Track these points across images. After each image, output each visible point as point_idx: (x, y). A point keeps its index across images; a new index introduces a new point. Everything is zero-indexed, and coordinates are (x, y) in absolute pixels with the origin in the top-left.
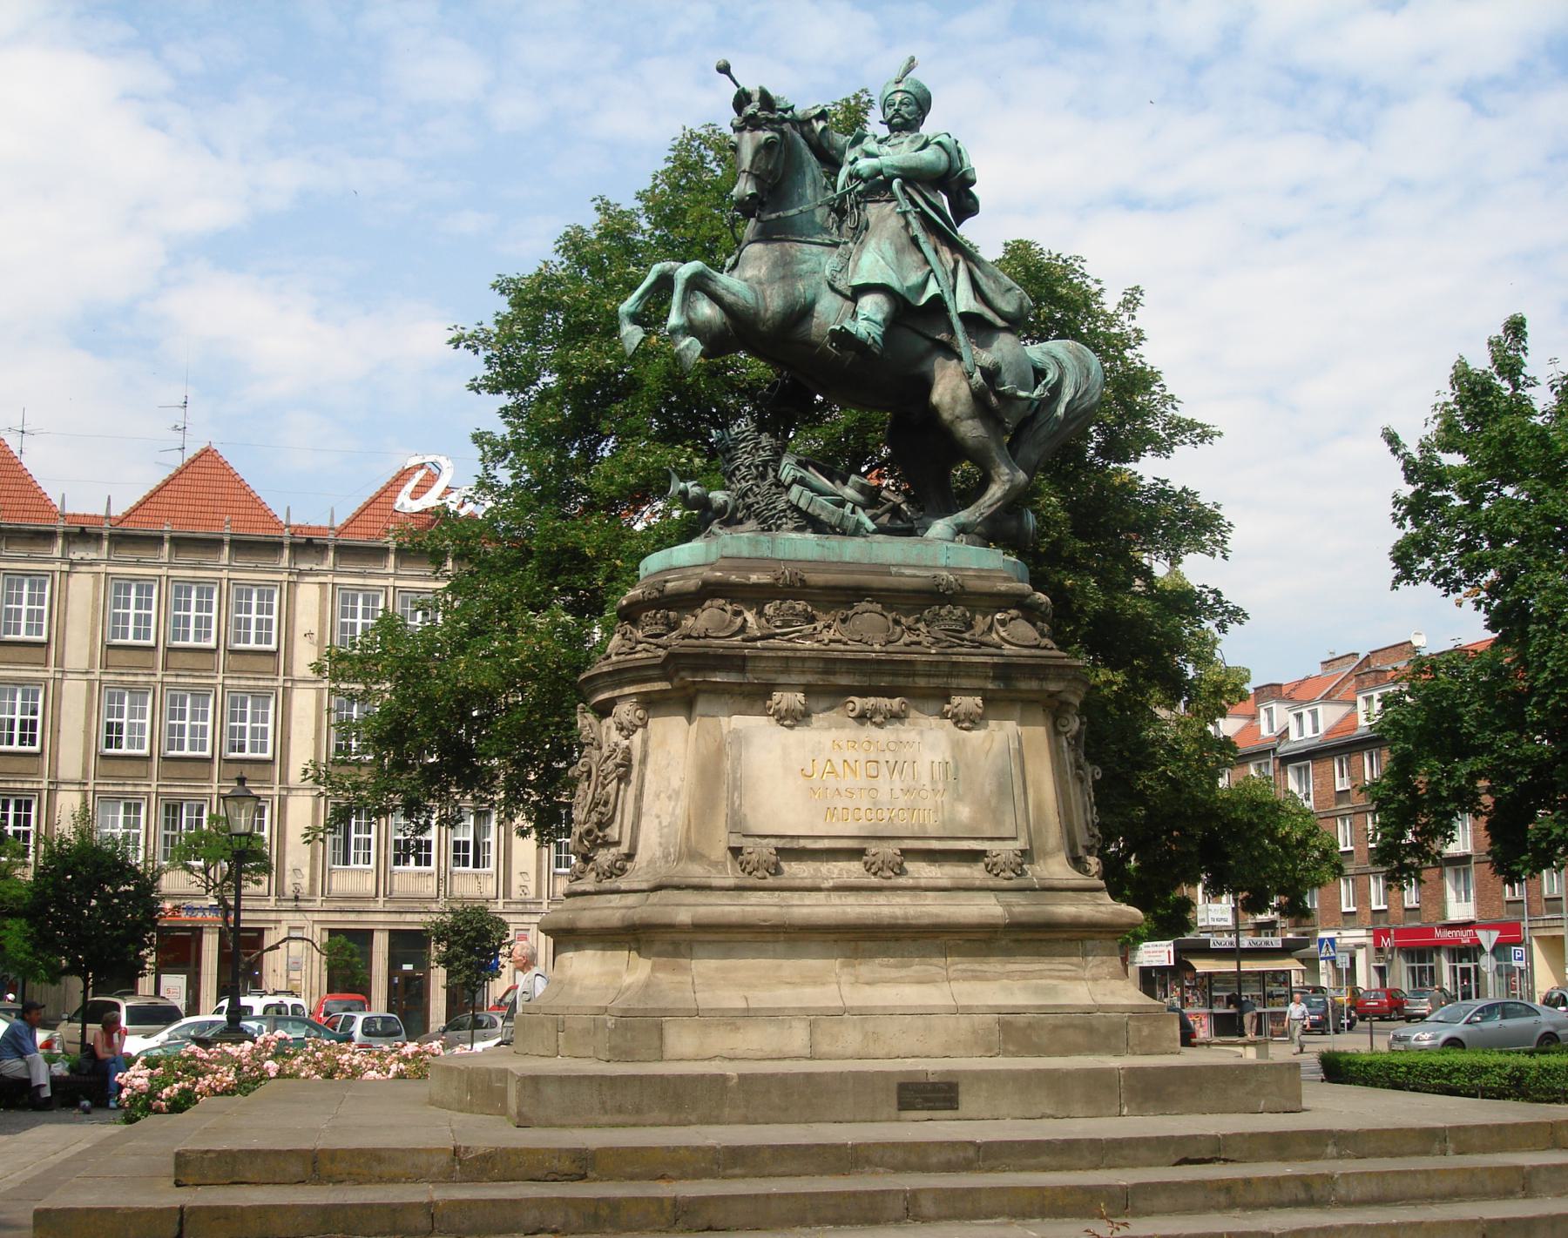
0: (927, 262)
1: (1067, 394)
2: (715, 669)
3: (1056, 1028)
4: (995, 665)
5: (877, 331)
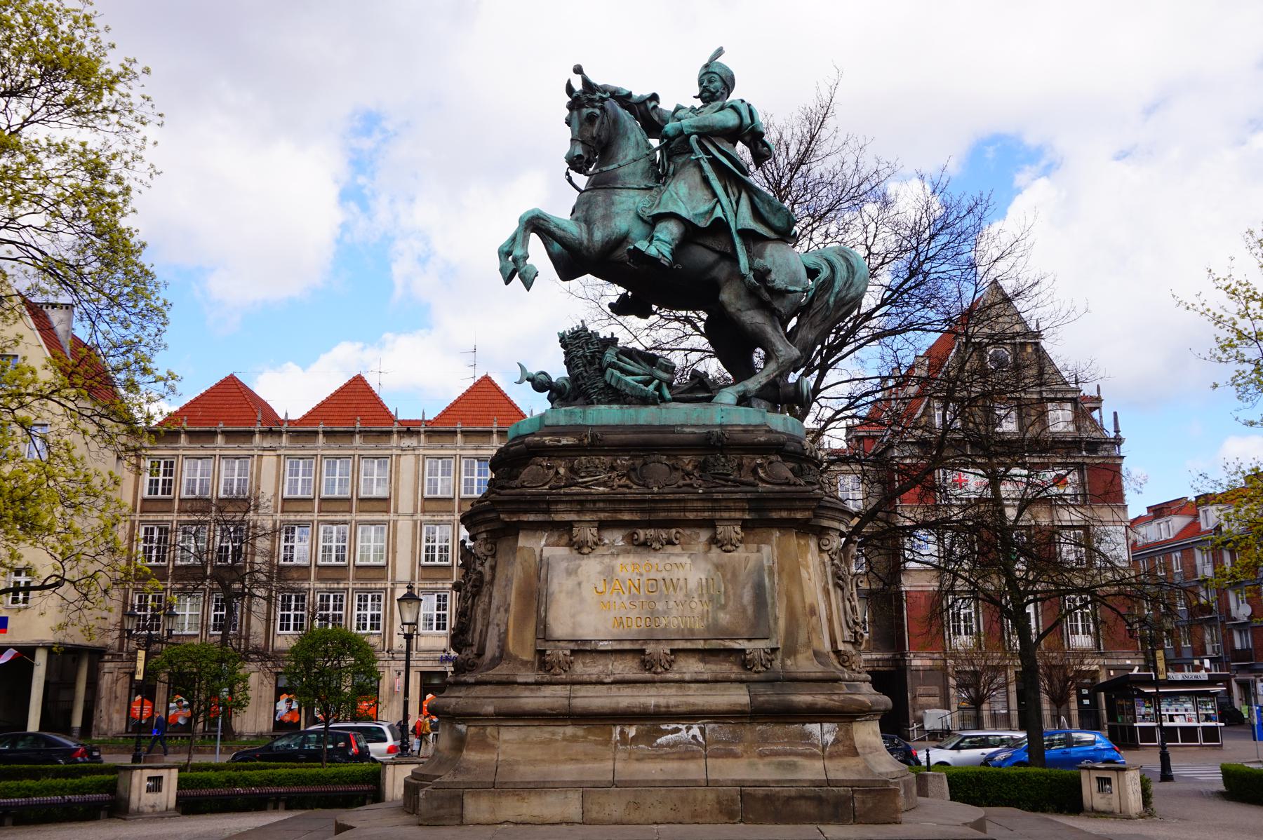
0: (715, 195)
1: (838, 285)
2: (526, 512)
3: (789, 799)
4: (748, 500)
5: (666, 250)
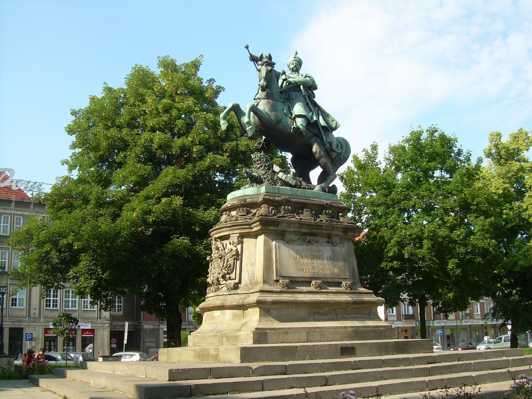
0: (311, 111)
2: (270, 225)
3: (368, 332)
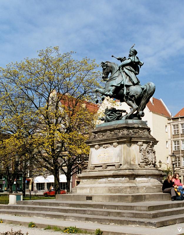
4: (116, 138)
